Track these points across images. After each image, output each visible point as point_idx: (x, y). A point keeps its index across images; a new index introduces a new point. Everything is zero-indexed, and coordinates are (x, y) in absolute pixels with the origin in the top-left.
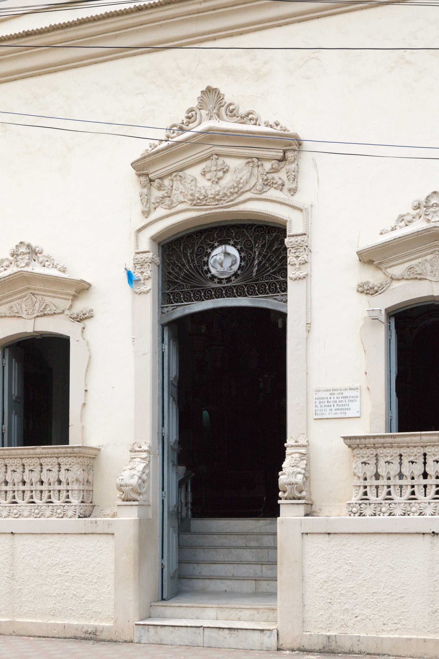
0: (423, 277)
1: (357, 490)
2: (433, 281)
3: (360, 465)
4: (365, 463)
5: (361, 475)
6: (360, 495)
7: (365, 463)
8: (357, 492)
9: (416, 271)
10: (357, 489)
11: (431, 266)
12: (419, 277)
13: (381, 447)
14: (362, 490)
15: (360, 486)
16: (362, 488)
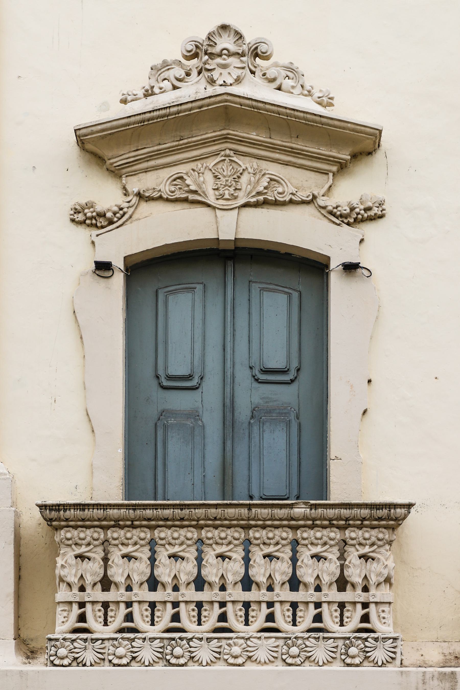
0: (199, 198)
1: (64, 610)
2: (218, 209)
3: (73, 561)
4: (81, 557)
5: (73, 579)
6: (72, 622)
7: (81, 557)
8: (65, 614)
9: (188, 186)
10: (66, 608)
11: (216, 177)
12: (191, 197)
13: (114, 526)
14: (76, 611)
15: (71, 603)
16: (75, 607)
